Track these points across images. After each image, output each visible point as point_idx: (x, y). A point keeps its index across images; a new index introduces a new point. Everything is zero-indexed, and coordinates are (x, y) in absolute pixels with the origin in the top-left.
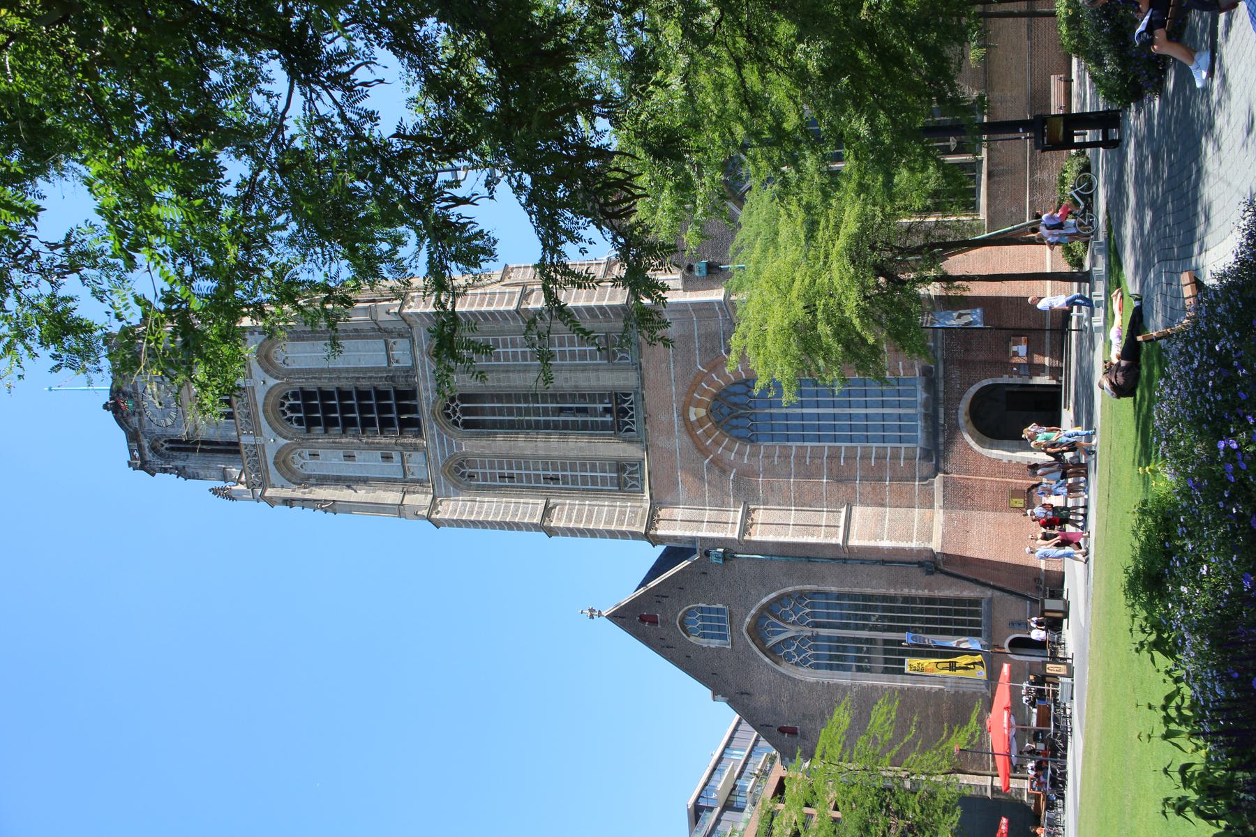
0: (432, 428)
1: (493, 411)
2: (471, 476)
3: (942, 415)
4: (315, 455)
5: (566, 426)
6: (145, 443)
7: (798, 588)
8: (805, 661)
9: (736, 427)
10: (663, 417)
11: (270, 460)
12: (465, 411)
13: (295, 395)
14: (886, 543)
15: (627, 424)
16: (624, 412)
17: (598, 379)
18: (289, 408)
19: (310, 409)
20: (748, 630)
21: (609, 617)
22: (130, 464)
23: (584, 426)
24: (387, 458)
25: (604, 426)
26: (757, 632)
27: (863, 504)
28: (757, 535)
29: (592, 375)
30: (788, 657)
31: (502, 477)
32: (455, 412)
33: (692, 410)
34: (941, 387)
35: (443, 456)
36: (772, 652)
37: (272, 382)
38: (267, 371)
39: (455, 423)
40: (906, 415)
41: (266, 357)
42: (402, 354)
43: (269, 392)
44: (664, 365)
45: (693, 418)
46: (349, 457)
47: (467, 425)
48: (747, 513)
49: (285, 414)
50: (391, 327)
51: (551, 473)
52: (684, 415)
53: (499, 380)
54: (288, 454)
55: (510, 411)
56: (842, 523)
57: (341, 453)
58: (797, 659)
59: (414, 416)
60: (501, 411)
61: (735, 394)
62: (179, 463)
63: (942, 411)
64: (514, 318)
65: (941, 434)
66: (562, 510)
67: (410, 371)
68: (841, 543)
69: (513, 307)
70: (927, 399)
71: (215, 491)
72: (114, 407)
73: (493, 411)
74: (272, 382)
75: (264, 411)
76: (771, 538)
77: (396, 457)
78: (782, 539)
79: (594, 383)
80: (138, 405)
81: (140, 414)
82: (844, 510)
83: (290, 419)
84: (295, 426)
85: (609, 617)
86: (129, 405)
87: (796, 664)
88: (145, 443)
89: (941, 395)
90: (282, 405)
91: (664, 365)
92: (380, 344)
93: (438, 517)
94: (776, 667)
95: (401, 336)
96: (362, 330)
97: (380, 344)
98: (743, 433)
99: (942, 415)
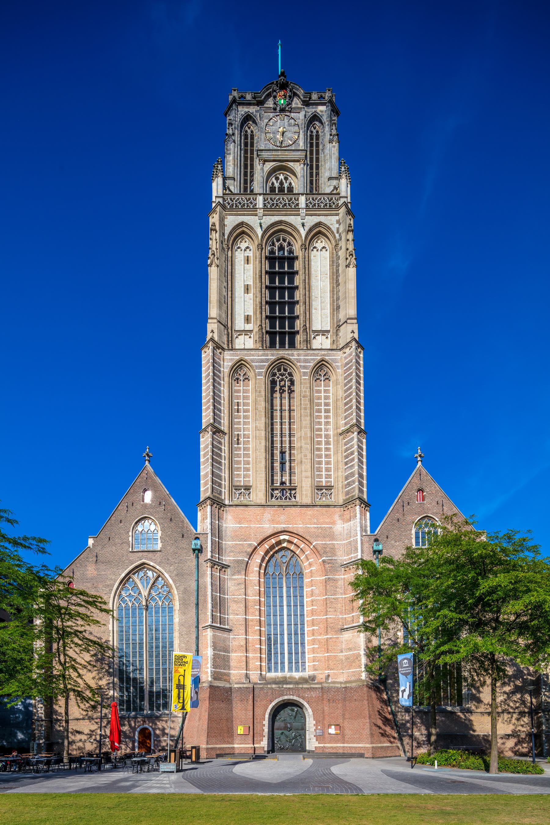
0: (272, 355)
3: (288, 686)
4: (247, 260)
10: (283, 518)
13: (291, 252)
17: (306, 477)
18: (281, 245)
19: (282, 259)
29: (309, 474)
34: (305, 686)
35: (253, 361)
40: (284, 666)
44: (316, 521)
46: (247, 289)
63: (291, 686)
65: (277, 686)
70: (295, 678)
89: (300, 686)
91: (316, 521)
99: (288, 686)
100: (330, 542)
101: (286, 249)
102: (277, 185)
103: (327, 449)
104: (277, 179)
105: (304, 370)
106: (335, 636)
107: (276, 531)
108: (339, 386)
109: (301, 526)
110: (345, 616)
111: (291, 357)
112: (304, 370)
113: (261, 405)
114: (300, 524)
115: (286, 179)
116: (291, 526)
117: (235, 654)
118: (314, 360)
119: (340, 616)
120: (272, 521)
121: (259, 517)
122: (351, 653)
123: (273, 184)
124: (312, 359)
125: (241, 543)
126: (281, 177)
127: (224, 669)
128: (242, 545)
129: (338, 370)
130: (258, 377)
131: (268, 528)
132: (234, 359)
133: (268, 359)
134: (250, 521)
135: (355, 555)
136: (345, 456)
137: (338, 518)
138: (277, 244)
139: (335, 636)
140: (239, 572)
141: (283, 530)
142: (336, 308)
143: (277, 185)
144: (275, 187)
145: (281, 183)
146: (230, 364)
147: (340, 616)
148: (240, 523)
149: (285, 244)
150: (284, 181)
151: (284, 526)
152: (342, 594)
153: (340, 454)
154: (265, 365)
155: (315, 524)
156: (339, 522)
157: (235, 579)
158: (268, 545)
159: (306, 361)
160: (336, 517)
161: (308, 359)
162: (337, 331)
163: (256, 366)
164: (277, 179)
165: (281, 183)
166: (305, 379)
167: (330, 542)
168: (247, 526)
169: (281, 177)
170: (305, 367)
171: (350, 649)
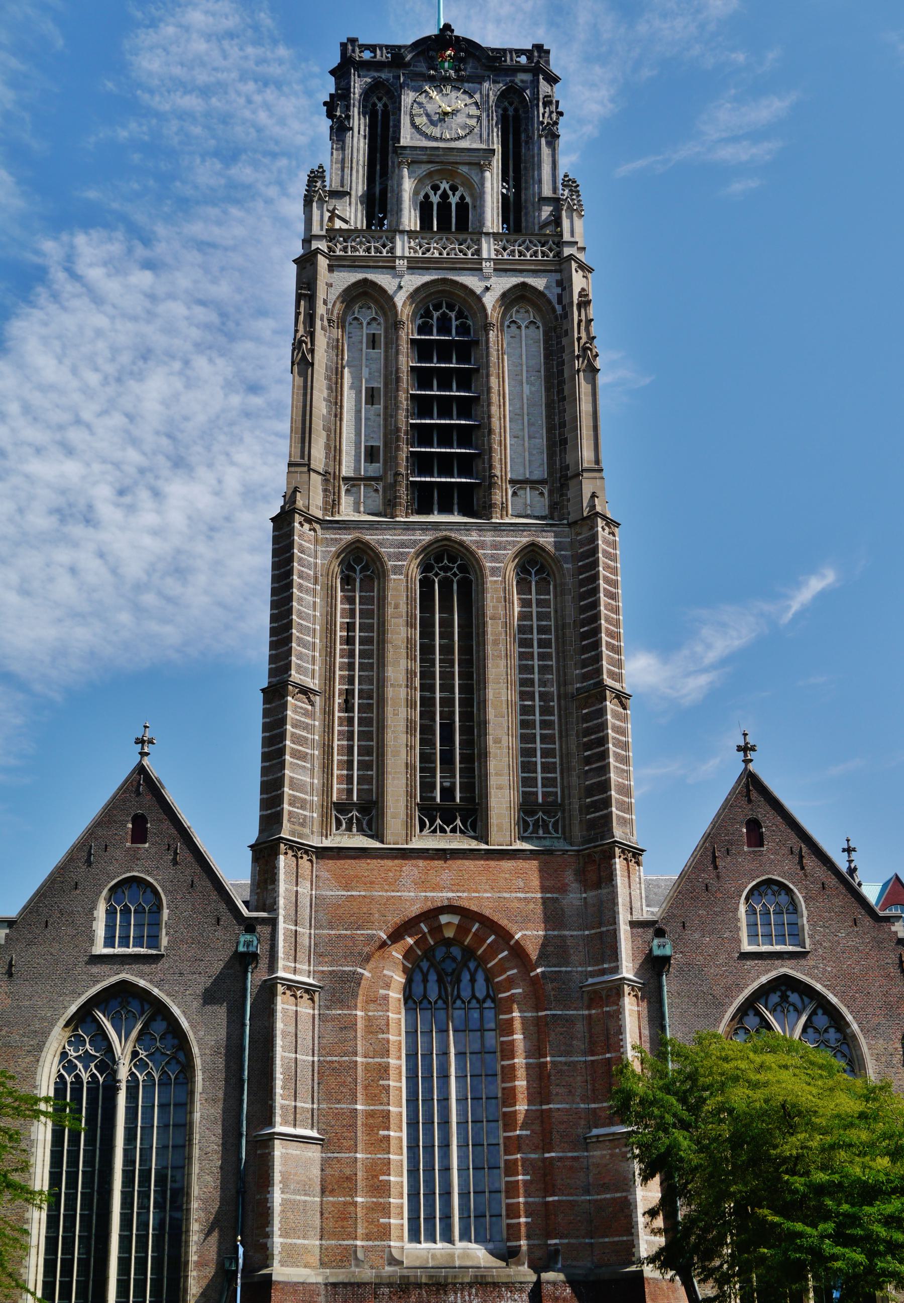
1: (446, 624)
5: (427, 731)
6: (384, 75)
7: (198, 1062)
8: (70, 1067)
9: (425, 981)
11: (371, 276)
12: (446, 586)
13: (463, 329)
14: (278, 1197)
15: (432, 823)
17: (500, 788)
20: (124, 982)
21: (141, 770)
22: (353, 41)
23: (426, 758)
24: (372, 454)
25: (427, 786)
26: (120, 998)
27: (325, 1164)
28: (283, 1004)
30: (76, 1041)
32: (446, 569)
33: (455, 919)
35: (381, 543)
36: (83, 1018)
44: (521, 884)
45: (444, 919)
47: (426, 584)
48: (309, 990)
49: (437, 307)
50: (571, 494)
52: (450, 909)
53: (496, 642)
54: (376, 302)
55: (447, 650)
56: (300, 1131)
57: (379, 384)
58: (72, 1053)
59: (436, 507)
60: (447, 634)
61: (473, 980)
64: (585, 677)
66: (306, 713)
68: (279, 1129)
69: (608, 681)
72: (445, 38)
73: (446, 624)
75: (444, 281)
76: (280, 1026)
77: (375, 469)
78: (279, 1042)
82: (314, 1134)
85: (141, 770)
87: (64, 1055)
88: (384, 75)
90: (451, 307)
91: (521, 884)
92: (540, 472)
93: (296, 525)
94: (62, 1022)
96: (564, 451)
97: (540, 472)
98: (418, 989)
100: (556, 933)
101: (454, 323)
102: (435, 199)
103: (545, 724)
104: (435, 188)
105: (493, 564)
106: (570, 1154)
107: (430, 905)
108: (568, 598)
109: (489, 895)
110: (593, 1106)
111: (465, 538)
112: (493, 564)
113: (399, 633)
114: (486, 891)
115: (454, 189)
116: (465, 894)
117: (331, 1199)
119: (582, 1106)
120: (422, 884)
121: (391, 874)
122: (608, 1196)
123: (427, 196)
124: (509, 543)
125: (349, 932)
126: (444, 185)
127: (304, 1238)
128: (352, 937)
129: (565, 566)
130: (393, 577)
132: (341, 539)
133: (415, 541)
134: (372, 883)
135: (612, 965)
136: (585, 744)
137: (571, 878)
138: (436, 315)
139: (570, 1154)
141: (446, 903)
143: (435, 199)
144: (432, 203)
145: (444, 196)
146: (333, 549)
147: (582, 1106)
148: (347, 888)
149: (453, 315)
150: (450, 193)
151: (450, 895)
152: (585, 1054)
153: (573, 739)
154: (409, 552)
155: (520, 890)
156: (575, 885)
157: (334, 1018)
159: (496, 546)
160: (569, 876)
161: (501, 543)
162: (562, 485)
164: (435, 188)
165: (444, 196)
166: (496, 582)
167: (556, 933)
168: (363, 893)
169: (444, 185)
170: (494, 558)
171: (605, 1188)
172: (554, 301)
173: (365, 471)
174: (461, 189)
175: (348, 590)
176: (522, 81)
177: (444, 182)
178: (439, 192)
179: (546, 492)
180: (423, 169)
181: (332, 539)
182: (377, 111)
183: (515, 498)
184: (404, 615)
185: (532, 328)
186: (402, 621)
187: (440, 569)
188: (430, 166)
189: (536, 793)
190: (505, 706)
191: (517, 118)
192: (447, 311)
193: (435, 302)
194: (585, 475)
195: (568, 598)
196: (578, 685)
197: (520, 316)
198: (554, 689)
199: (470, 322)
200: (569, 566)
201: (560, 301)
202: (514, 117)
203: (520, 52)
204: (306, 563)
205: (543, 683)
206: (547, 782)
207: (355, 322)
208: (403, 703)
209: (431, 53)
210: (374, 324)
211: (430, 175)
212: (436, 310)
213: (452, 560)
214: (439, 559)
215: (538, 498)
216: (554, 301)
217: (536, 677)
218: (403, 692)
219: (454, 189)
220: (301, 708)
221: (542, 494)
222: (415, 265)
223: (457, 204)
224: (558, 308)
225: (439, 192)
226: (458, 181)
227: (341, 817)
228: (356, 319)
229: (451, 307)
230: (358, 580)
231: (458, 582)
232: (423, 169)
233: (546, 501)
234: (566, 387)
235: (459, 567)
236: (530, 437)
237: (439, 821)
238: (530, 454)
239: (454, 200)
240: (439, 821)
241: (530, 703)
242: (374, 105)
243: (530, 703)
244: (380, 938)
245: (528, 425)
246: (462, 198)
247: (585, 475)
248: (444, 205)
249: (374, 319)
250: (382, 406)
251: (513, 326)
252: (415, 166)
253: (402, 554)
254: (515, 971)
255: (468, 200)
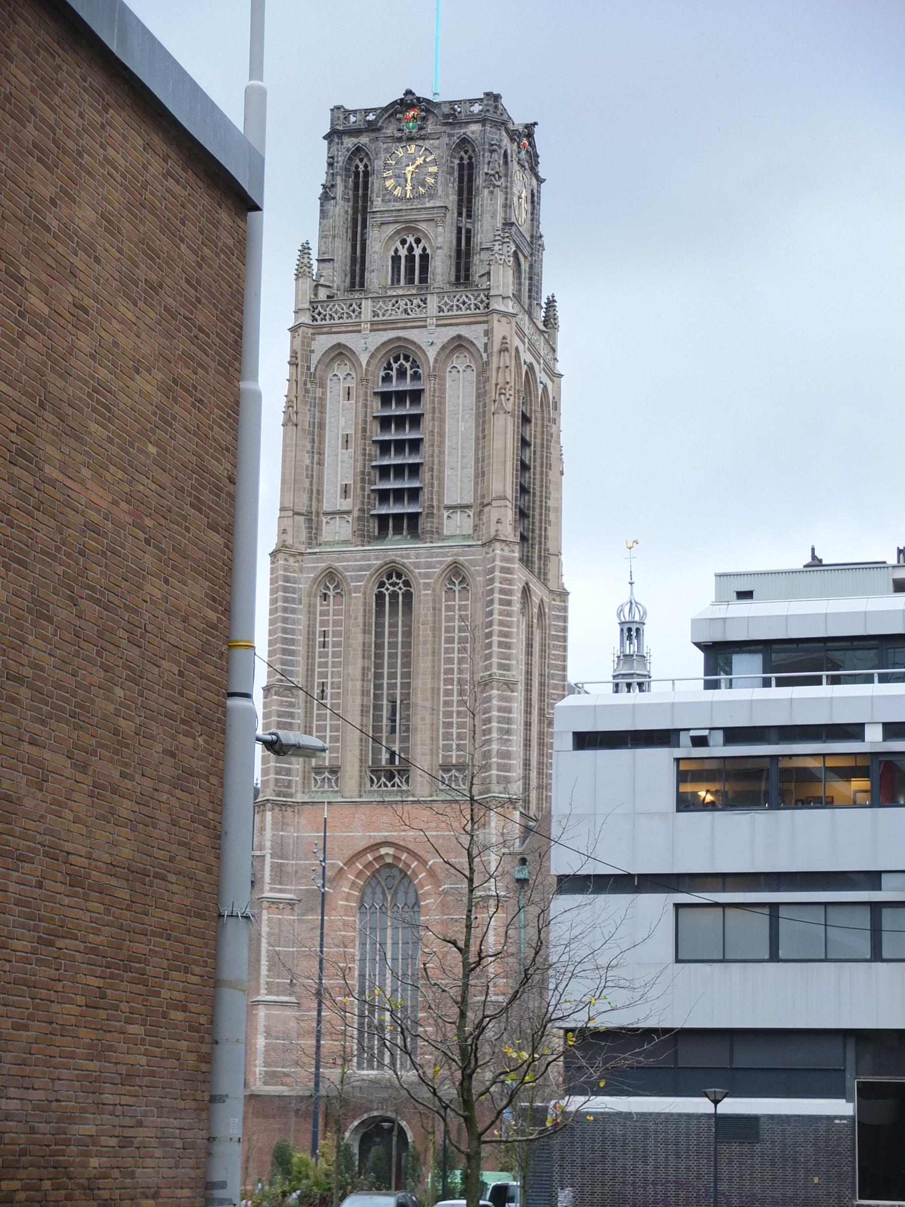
2: (325, 597)
6: (364, 140)
12: (394, 595)
15: (379, 779)
16: (390, 777)
17: (424, 754)
18: (401, 365)
29: (427, 748)
31: (325, 634)
33: (391, 851)
35: (346, 569)
37: (432, 353)
38: (443, 348)
39: (382, 585)
41: (460, 346)
42: (457, 525)
43: (420, 348)
45: (383, 851)
47: (380, 597)
51: (329, 691)
53: (425, 643)
61: (406, 893)
62: (339, 190)
67: (437, 533)
71: (305, 250)
72: (409, 102)
74: (432, 353)
79: (419, 749)
80: (411, 139)
81: (399, 140)
83: (389, 367)
84: (382, 373)
86: (409, 122)
95: (476, 528)
101: (409, 372)
102: (403, 252)
104: (403, 242)
107: (373, 842)
108: (479, 605)
111: (405, 561)
115: (418, 241)
116: (396, 834)
118: (441, 562)
123: (396, 250)
124: (438, 562)
126: (411, 239)
130: (354, 595)
131: (361, 837)
134: (335, 827)
138: (395, 366)
140: (312, 910)
141: (383, 840)
142: (481, 475)
144: (400, 257)
145: (411, 249)
149: (408, 365)
150: (414, 245)
158: (361, 864)
159: (429, 565)
161: (431, 562)
163: (351, 576)
165: (411, 249)
169: (411, 239)
170: (427, 576)
172: (482, 350)
173: (341, 505)
174: (423, 241)
175: (326, 605)
176: (473, 133)
177: (410, 235)
178: (406, 246)
179: (471, 514)
180: (391, 229)
181: (312, 567)
182: (359, 172)
183: (450, 520)
184: (361, 624)
185: (469, 370)
186: (359, 629)
187: (391, 584)
188: (397, 225)
189: (451, 756)
190: (429, 692)
191: (471, 166)
192: (404, 362)
193: (394, 355)
194: (494, 503)
195: (479, 605)
196: (481, 674)
197: (460, 361)
198: (467, 676)
199: (420, 371)
200: (481, 579)
201: (486, 351)
202: (468, 163)
203: (472, 102)
204: (291, 589)
205: (460, 671)
206: (459, 748)
207: (335, 378)
208: (359, 693)
209: (399, 116)
210: (349, 378)
211: (398, 232)
212: (395, 362)
213: (399, 576)
214: (389, 577)
215: (466, 519)
216: (482, 350)
217: (455, 666)
218: (358, 684)
219: (418, 241)
220: (286, 702)
221: (469, 516)
222: (377, 326)
223: (420, 255)
224: (484, 355)
225: (406, 246)
226: (420, 235)
227: (317, 778)
228: (335, 375)
229: (407, 358)
230: (331, 597)
231: (403, 594)
232: (391, 229)
233: (471, 522)
234: (486, 426)
235: (404, 582)
236: (462, 468)
237: (383, 779)
238: (461, 481)
239: (417, 252)
240: (383, 779)
241: (450, 687)
242: (357, 167)
243: (450, 687)
244: (339, 865)
245: (462, 457)
246: (424, 249)
247: (494, 503)
248: (410, 258)
249: (349, 374)
250: (353, 450)
251: (454, 370)
252: (384, 227)
253: (360, 576)
254: (430, 887)
255: (428, 251)
